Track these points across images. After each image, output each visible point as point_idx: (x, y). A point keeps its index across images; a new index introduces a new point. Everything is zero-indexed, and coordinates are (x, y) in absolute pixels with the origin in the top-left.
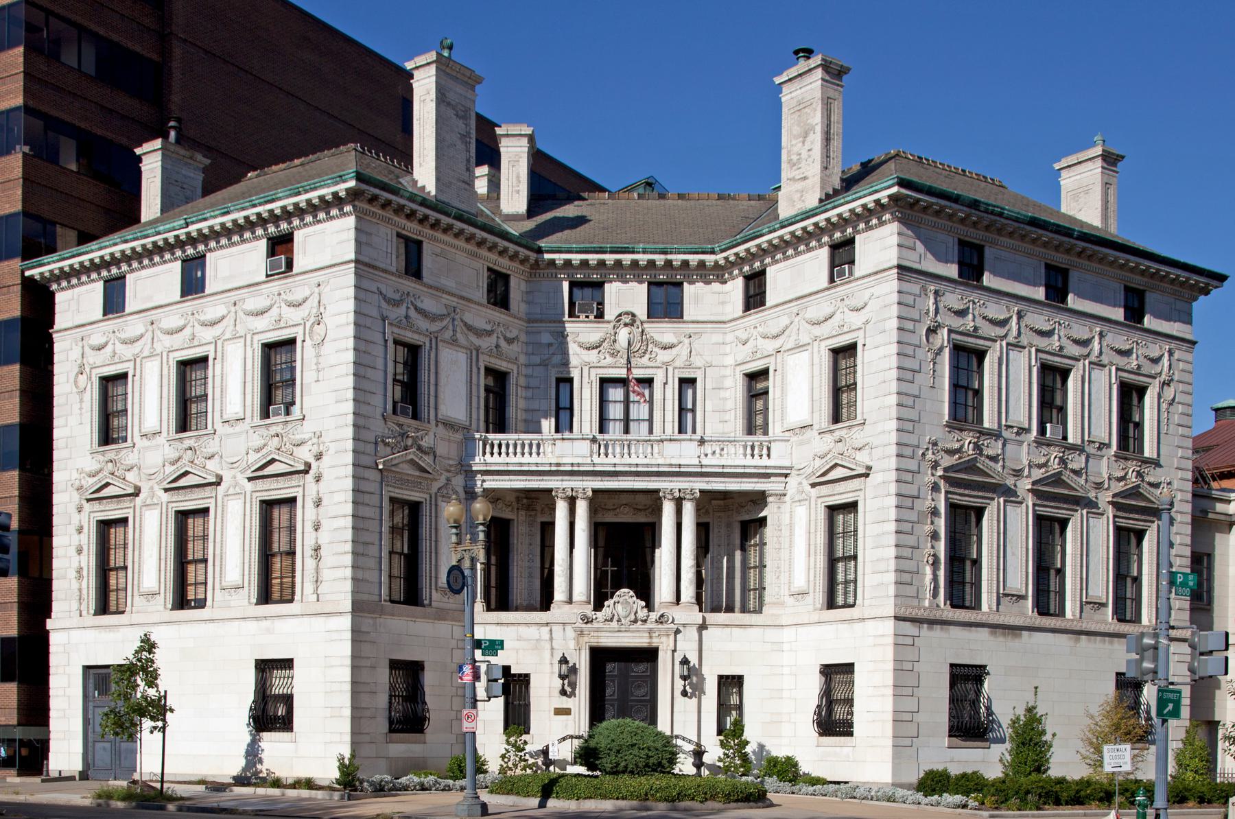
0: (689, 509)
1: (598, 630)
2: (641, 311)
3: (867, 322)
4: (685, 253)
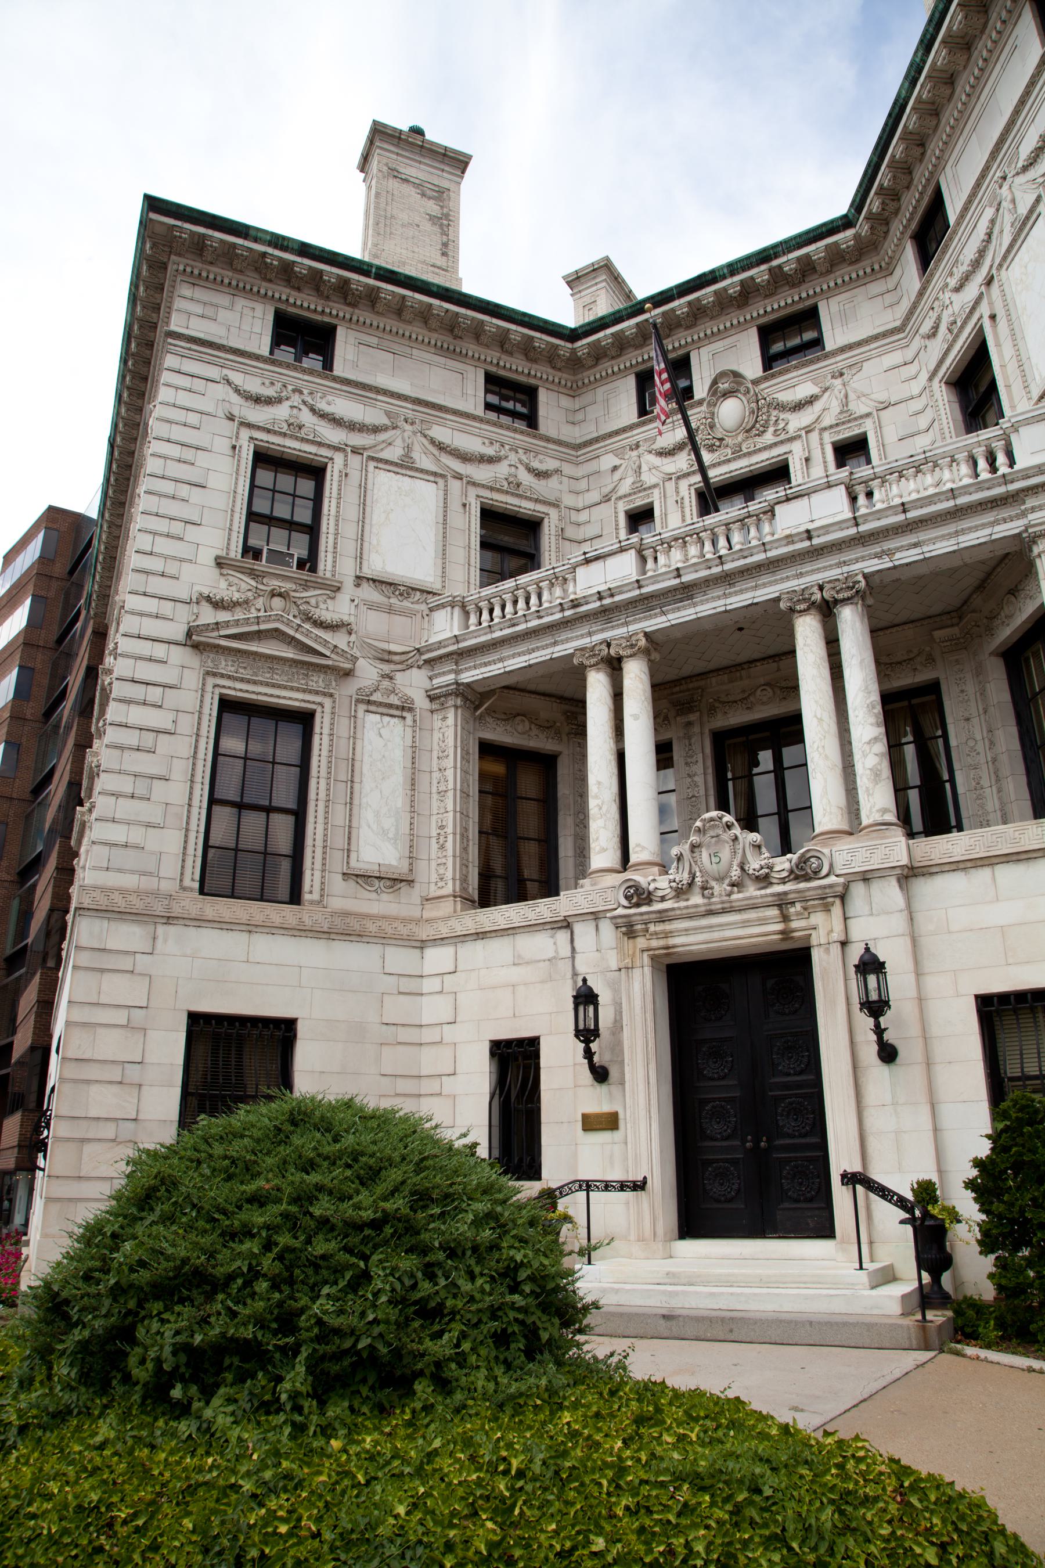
0: (851, 624)
1: (663, 917)
2: (751, 366)
4: (800, 246)
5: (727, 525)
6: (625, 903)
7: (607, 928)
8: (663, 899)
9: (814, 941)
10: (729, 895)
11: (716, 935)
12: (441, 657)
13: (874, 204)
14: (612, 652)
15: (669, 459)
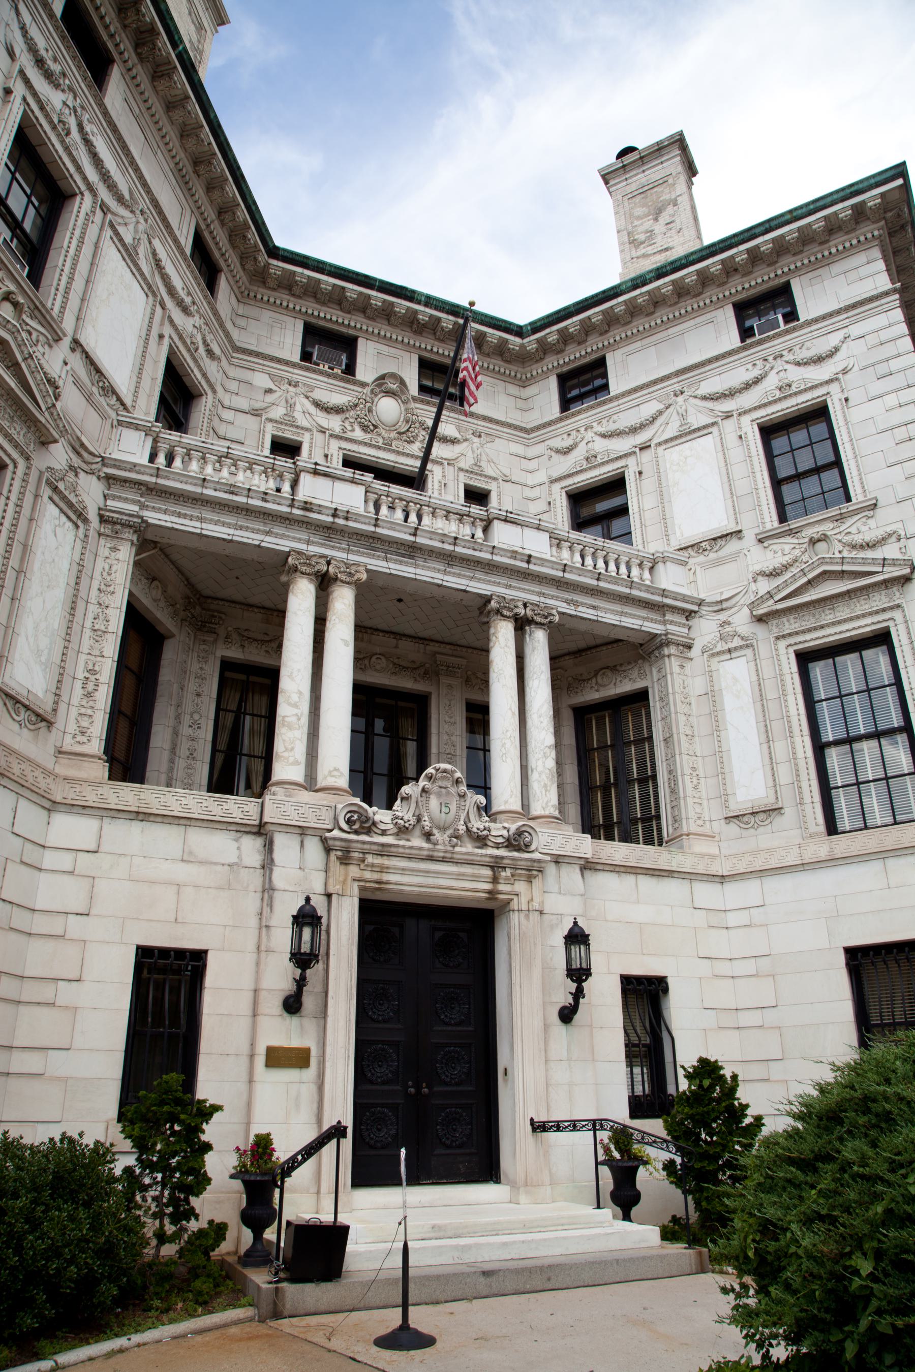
1: (384, 851)
3: (845, 371)
5: (449, 512)
6: (345, 826)
7: (313, 847)
8: (384, 833)
9: (514, 905)
10: (454, 847)
11: (431, 881)
12: (125, 481)
13: (551, 334)
14: (332, 570)
15: (324, 414)
